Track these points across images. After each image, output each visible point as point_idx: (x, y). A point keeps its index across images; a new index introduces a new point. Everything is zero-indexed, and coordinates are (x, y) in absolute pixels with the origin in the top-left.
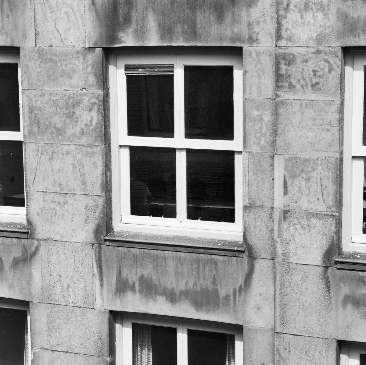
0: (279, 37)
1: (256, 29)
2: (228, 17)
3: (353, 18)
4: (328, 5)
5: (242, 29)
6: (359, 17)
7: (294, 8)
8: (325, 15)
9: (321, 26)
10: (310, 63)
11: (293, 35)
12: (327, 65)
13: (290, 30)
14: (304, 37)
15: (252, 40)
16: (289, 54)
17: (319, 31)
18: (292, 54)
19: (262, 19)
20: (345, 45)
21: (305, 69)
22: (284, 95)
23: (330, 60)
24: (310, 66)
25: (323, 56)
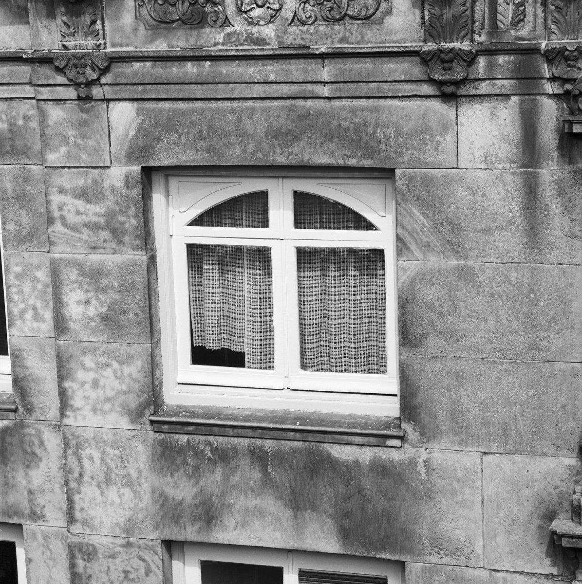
0: (71, 520)
1: (41, 500)
3: (175, 501)
4: (138, 479)
6: (183, 500)
7: (90, 480)
8: (135, 493)
9: (130, 508)
10: (118, 560)
11: (92, 518)
12: (143, 564)
13: (87, 511)
14: (108, 522)
15: (35, 516)
16: (88, 545)
17: (128, 514)
18: (92, 545)
19: (47, 486)
20: (166, 538)
21: (112, 568)
23: (146, 558)
24: (118, 564)
25: (135, 551)
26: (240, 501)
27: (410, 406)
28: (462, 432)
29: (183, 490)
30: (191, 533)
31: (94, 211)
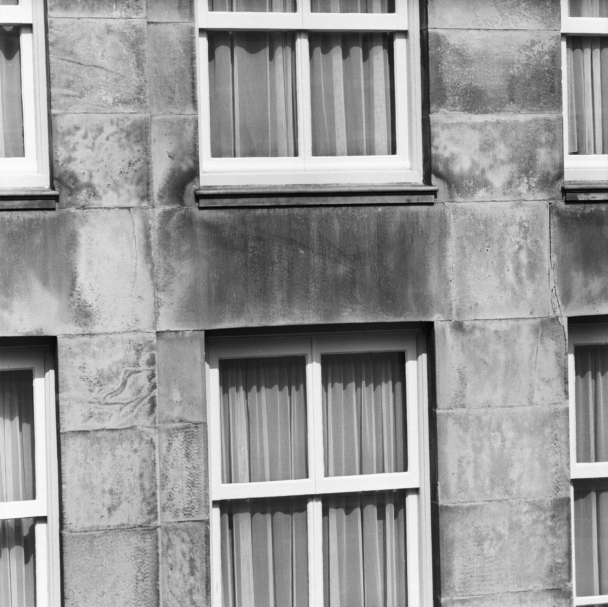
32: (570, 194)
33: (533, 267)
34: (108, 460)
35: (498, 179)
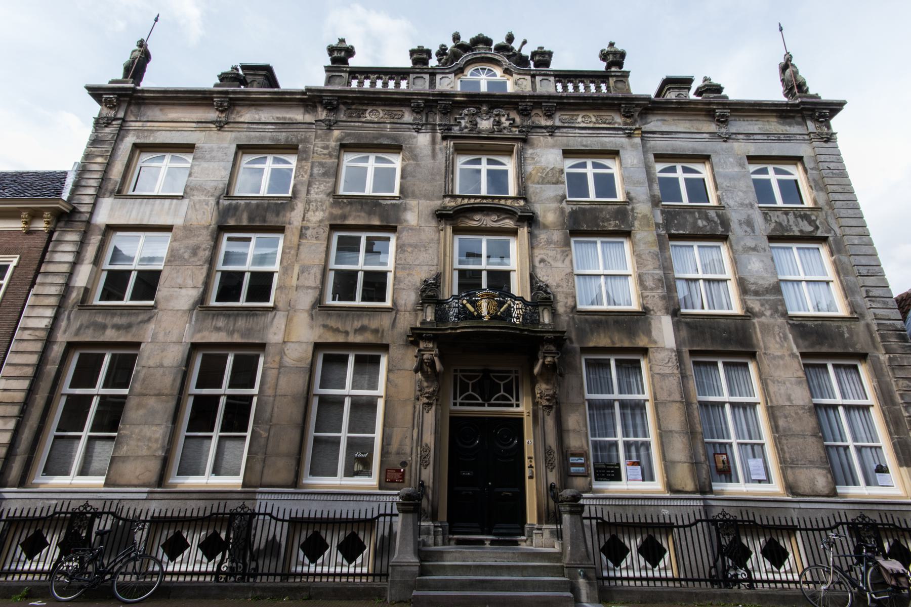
0: (303, 220)
2: (281, 214)
5: (287, 220)
15: (290, 224)
22: (304, 241)
26: (354, 214)
27: (401, 192)
28: (414, 196)
29: (337, 211)
30: (339, 222)
31: (325, 151)
32: (791, 318)
33: (785, 338)
34: (667, 381)
35: (768, 313)
